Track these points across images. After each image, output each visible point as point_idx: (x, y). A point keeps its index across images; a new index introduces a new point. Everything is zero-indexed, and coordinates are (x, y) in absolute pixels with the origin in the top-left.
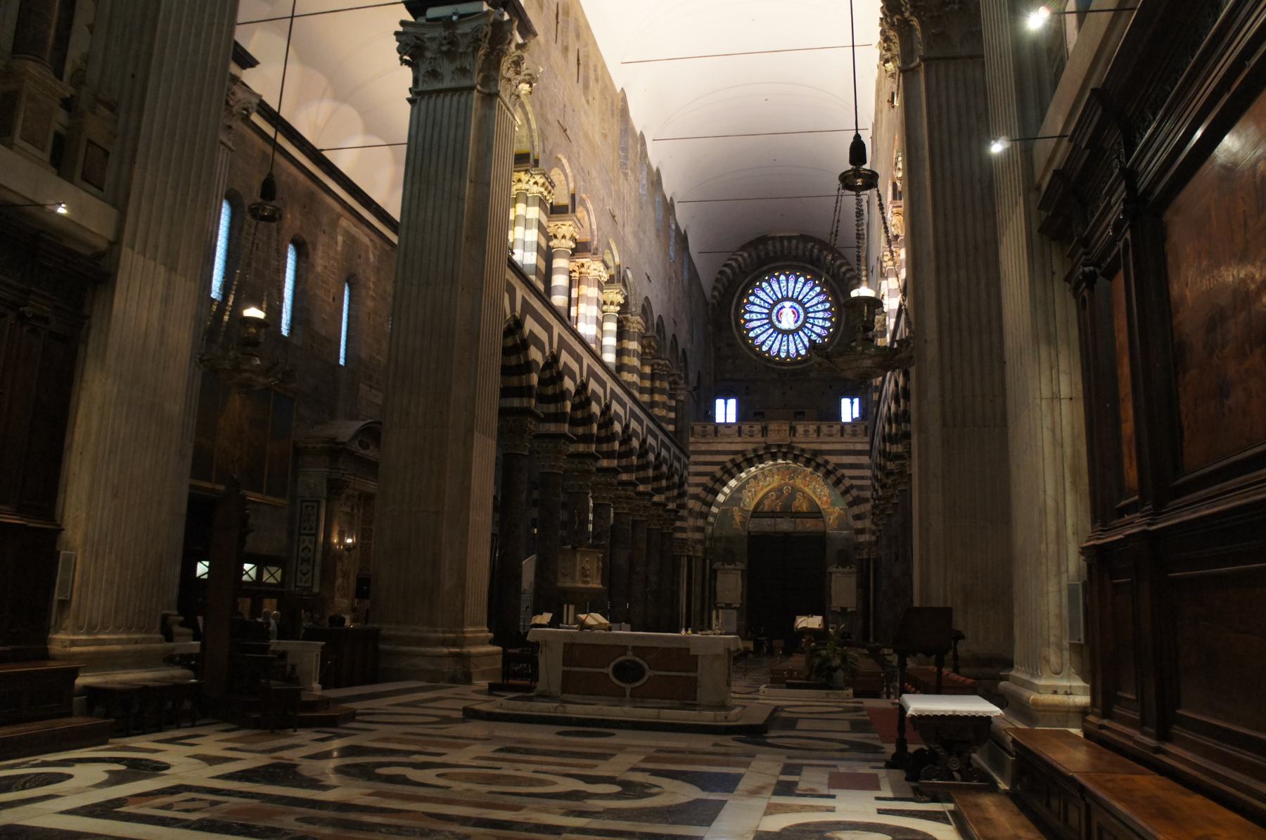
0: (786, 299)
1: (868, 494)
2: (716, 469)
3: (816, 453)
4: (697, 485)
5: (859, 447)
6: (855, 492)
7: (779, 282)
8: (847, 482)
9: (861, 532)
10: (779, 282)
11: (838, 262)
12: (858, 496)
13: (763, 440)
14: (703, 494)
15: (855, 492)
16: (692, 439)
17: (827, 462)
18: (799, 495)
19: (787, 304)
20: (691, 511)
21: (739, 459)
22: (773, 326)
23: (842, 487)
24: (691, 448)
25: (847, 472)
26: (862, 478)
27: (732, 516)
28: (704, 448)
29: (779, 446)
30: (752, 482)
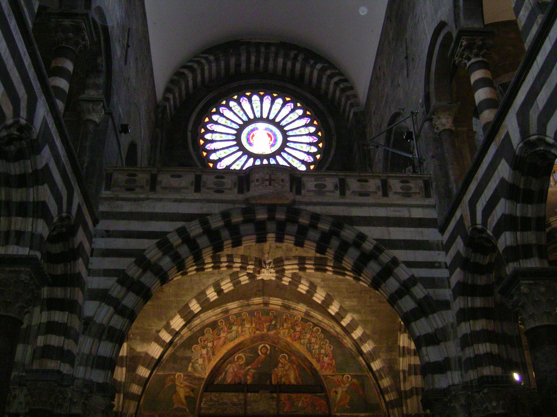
0: (261, 119)
1: (446, 293)
2: (148, 246)
3: (340, 222)
4: (107, 273)
5: (417, 213)
6: (419, 291)
8: (403, 273)
9: (442, 367)
10: (250, 101)
11: (329, 72)
12: (427, 298)
13: (241, 197)
14: (117, 291)
15: (419, 291)
16: (105, 193)
17: (362, 237)
18: (283, 359)
19: (261, 126)
20: (88, 322)
21: (195, 229)
22: (242, 148)
23: (392, 284)
24: (103, 208)
25: (402, 255)
26: (431, 265)
27: (174, 387)
28: (127, 207)
29: (271, 209)
30: (209, 334)
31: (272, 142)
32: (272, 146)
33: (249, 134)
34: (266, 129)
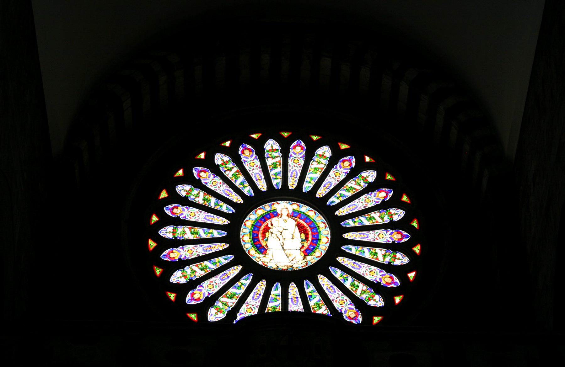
0: (284, 193)
7: (261, 155)
10: (261, 155)
31: (306, 245)
32: (307, 252)
33: (256, 226)
34: (294, 215)
